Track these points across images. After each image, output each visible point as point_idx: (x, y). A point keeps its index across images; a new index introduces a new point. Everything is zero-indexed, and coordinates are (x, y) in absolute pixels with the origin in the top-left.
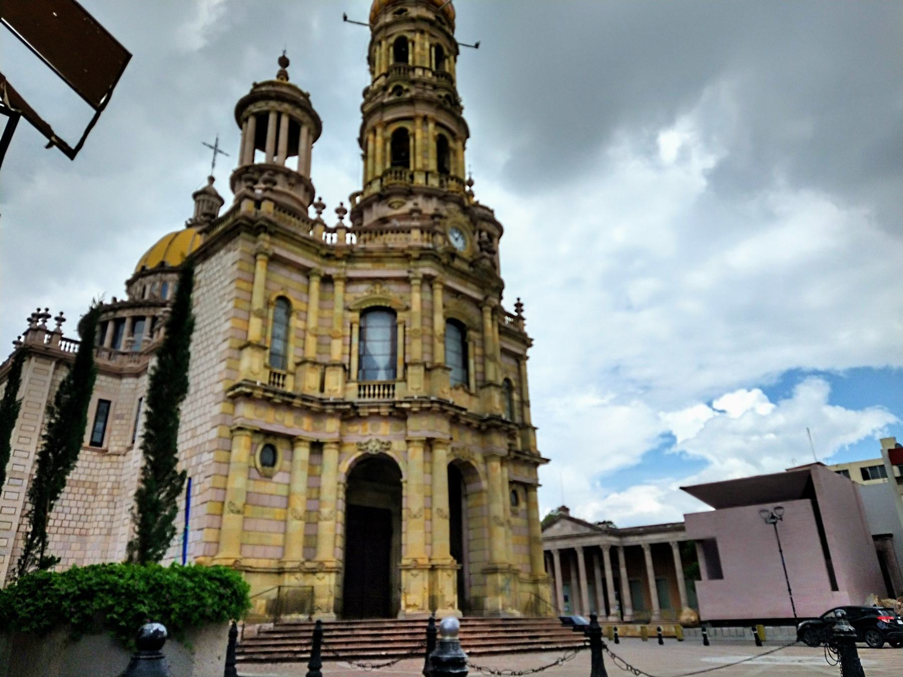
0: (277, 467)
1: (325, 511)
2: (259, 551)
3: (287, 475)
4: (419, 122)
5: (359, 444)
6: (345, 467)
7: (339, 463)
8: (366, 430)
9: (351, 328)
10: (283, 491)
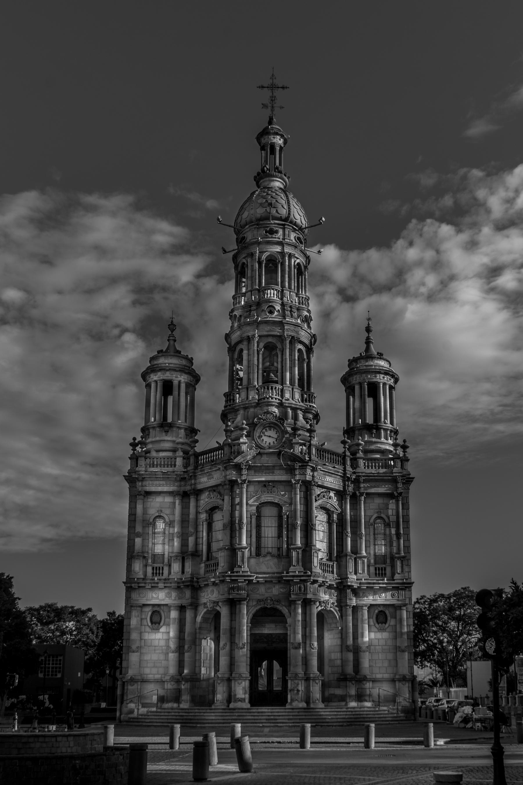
0: (162, 624)
1: (186, 647)
2: (154, 671)
3: (168, 627)
4: (245, 343)
5: (205, 604)
6: (199, 619)
7: (195, 617)
8: (208, 595)
9: (203, 525)
10: (165, 637)
